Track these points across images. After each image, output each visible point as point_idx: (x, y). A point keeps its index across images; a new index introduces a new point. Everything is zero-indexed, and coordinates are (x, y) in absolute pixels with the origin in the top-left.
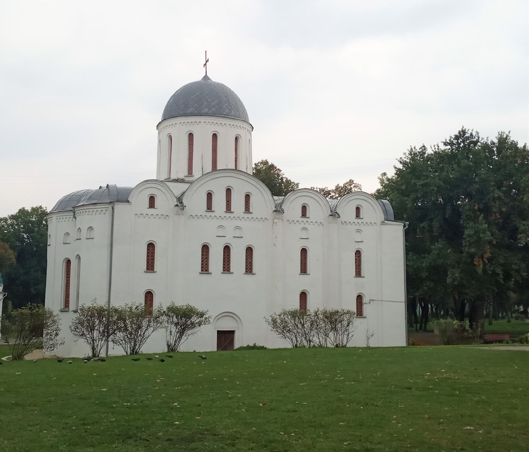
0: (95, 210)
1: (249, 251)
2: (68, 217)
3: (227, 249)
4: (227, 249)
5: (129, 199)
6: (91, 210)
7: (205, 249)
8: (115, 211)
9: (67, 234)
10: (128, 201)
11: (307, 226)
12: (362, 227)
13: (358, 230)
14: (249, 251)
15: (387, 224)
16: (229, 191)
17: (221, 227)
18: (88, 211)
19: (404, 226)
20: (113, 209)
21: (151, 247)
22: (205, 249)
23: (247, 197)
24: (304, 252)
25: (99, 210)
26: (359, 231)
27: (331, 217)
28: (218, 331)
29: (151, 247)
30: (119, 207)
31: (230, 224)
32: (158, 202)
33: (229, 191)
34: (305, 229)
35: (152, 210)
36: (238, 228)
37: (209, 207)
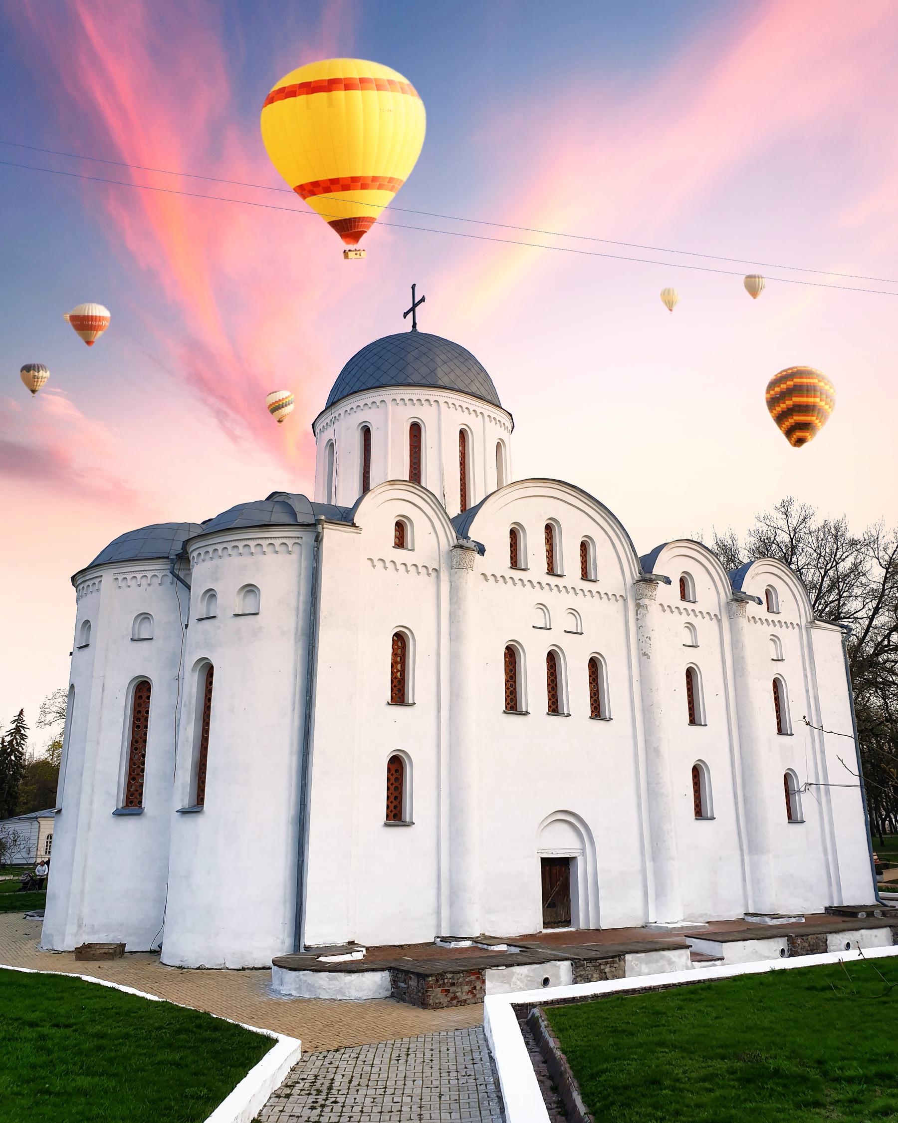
1: (594, 665)
2: (149, 574)
7: (511, 654)
9: (145, 617)
11: (691, 619)
12: (777, 630)
13: (772, 637)
15: (819, 627)
21: (400, 641)
22: (511, 654)
23: (584, 546)
24: (690, 674)
27: (735, 605)
28: (542, 859)
31: (558, 602)
36: (573, 612)
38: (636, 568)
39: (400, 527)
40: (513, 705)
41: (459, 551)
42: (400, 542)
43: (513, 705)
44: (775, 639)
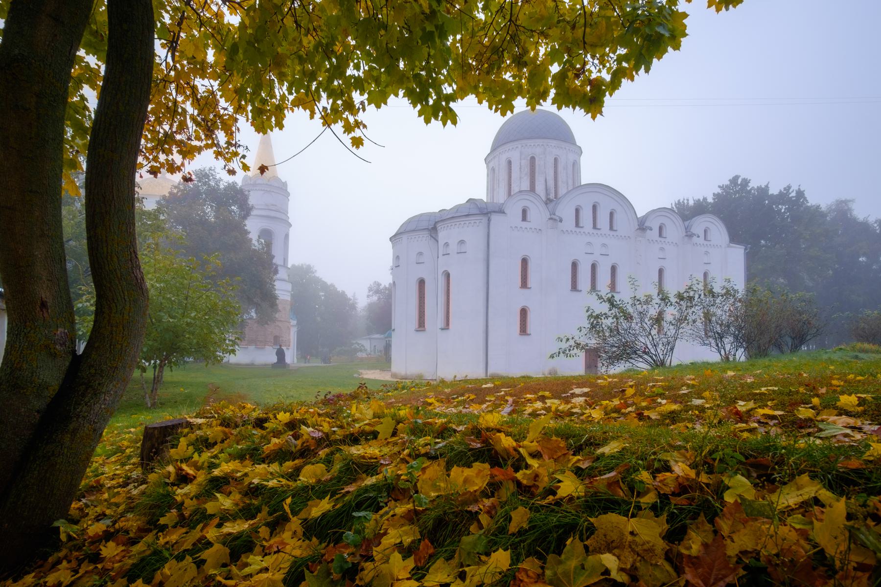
0: (467, 222)
1: (614, 269)
3: (594, 267)
4: (594, 267)
5: (505, 211)
6: (462, 223)
7: (574, 265)
8: (492, 223)
10: (504, 213)
14: (614, 269)
16: (594, 208)
17: (589, 243)
18: (458, 223)
19: (745, 249)
20: (489, 220)
21: (525, 262)
22: (574, 265)
23: (611, 214)
25: (472, 222)
26: (707, 253)
27: (686, 238)
29: (525, 262)
30: (495, 218)
32: (531, 215)
33: (594, 208)
34: (662, 249)
35: (525, 223)
36: (604, 245)
37: (577, 225)
38: (636, 224)
39: (524, 212)
40: (574, 287)
41: (551, 221)
42: (524, 218)
43: (574, 287)
44: (707, 253)
